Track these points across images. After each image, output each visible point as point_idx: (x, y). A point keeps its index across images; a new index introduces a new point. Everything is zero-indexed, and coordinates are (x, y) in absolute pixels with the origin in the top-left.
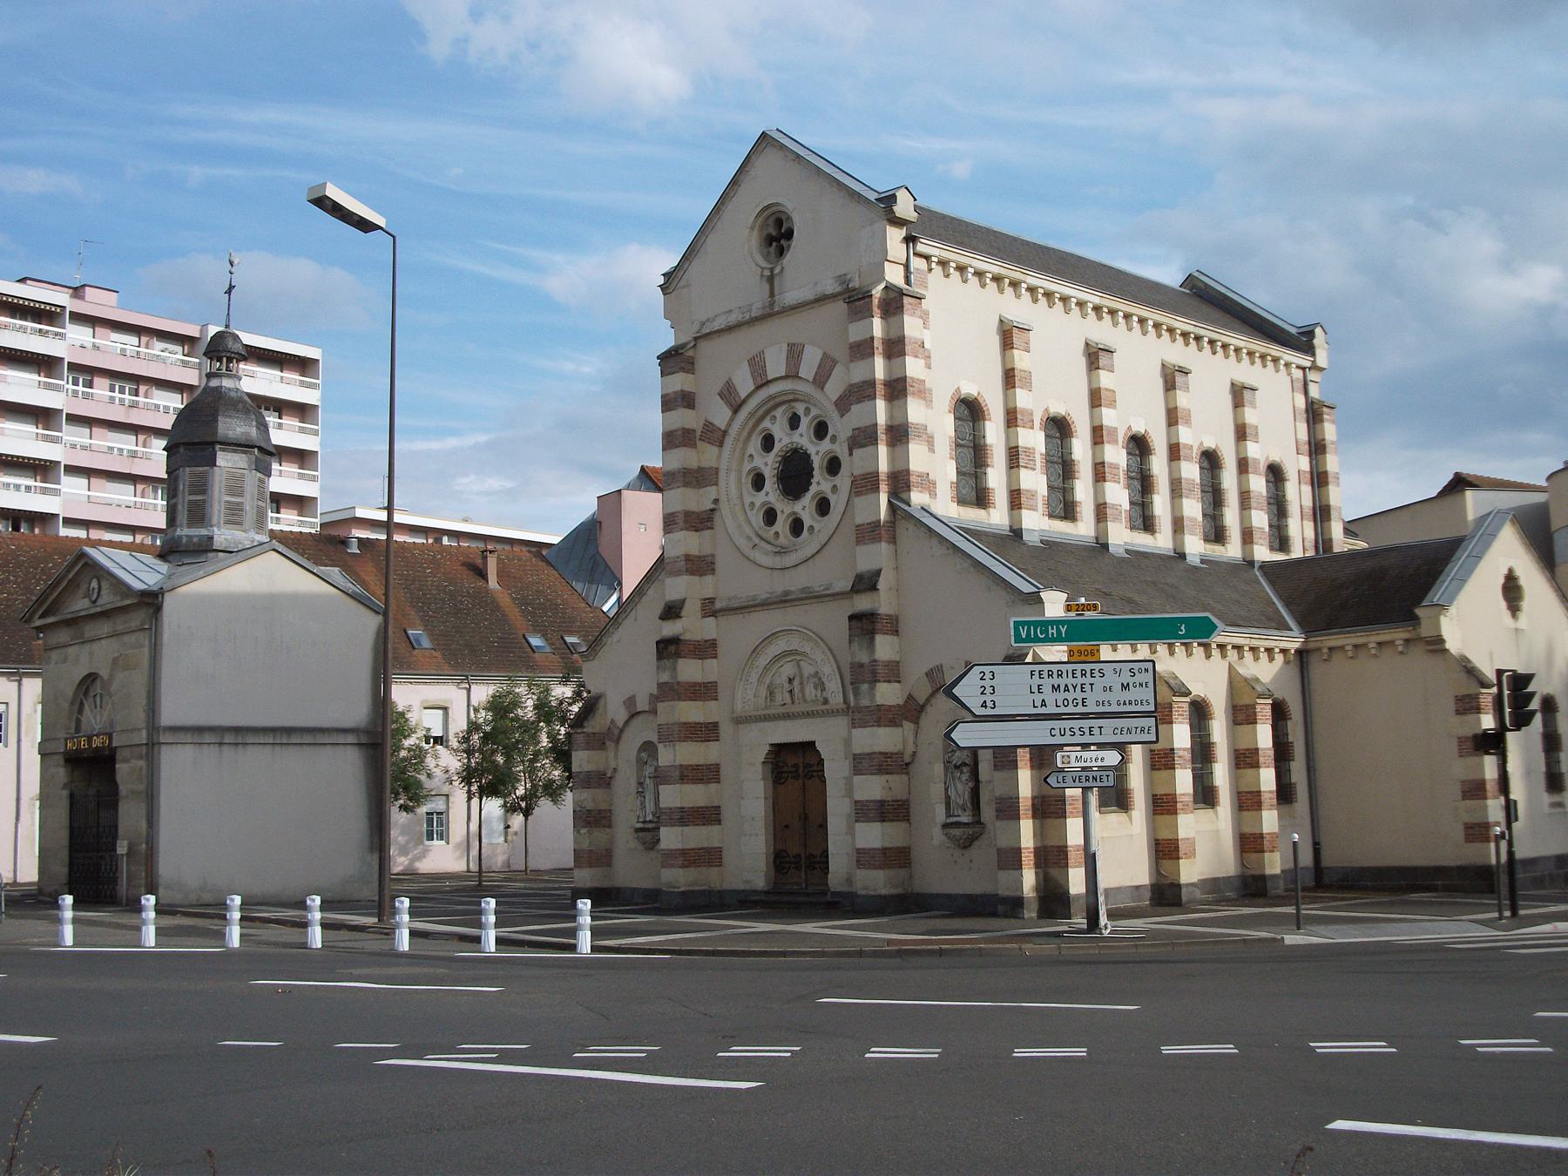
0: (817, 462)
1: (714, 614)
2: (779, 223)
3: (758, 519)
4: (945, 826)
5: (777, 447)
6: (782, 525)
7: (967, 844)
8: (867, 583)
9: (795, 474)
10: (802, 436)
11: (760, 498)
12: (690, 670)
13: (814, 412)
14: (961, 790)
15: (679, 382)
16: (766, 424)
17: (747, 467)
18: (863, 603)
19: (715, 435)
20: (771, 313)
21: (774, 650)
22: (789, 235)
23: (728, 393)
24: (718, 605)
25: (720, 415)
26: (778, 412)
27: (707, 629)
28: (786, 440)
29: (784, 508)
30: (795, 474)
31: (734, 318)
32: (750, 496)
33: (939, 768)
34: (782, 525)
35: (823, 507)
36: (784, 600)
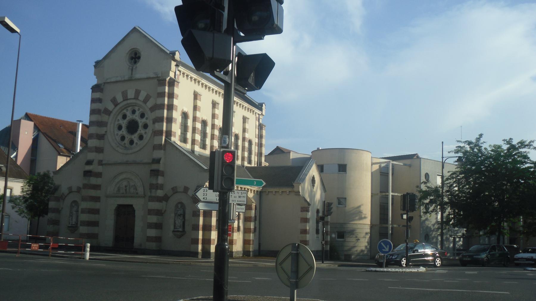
0: (140, 125)
1: (102, 165)
2: (136, 54)
3: (118, 139)
4: (174, 231)
5: (128, 118)
6: (127, 141)
7: (180, 237)
8: (157, 161)
9: (133, 127)
10: (136, 117)
11: (120, 133)
12: (93, 181)
13: (141, 110)
14: (179, 222)
15: (98, 95)
16: (125, 111)
17: (117, 123)
18: (155, 167)
19: (107, 112)
20: (130, 80)
21: (121, 177)
22: (139, 58)
23: (114, 102)
24: (104, 162)
25: (111, 107)
26: (129, 109)
27: (99, 169)
28: (131, 117)
29: (128, 137)
30: (133, 127)
31: (119, 79)
32: (116, 132)
33: (173, 215)
34: (127, 141)
35: (141, 137)
36: (127, 163)
